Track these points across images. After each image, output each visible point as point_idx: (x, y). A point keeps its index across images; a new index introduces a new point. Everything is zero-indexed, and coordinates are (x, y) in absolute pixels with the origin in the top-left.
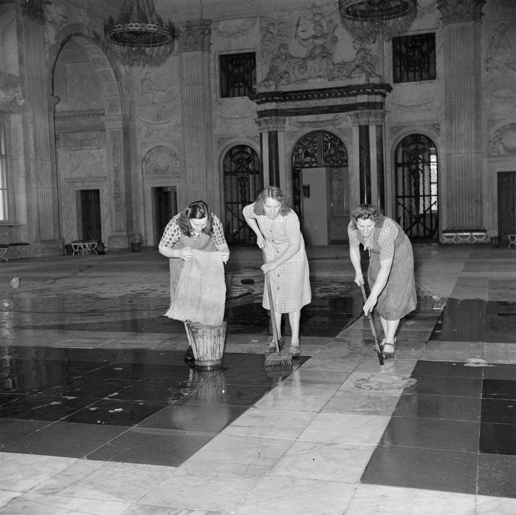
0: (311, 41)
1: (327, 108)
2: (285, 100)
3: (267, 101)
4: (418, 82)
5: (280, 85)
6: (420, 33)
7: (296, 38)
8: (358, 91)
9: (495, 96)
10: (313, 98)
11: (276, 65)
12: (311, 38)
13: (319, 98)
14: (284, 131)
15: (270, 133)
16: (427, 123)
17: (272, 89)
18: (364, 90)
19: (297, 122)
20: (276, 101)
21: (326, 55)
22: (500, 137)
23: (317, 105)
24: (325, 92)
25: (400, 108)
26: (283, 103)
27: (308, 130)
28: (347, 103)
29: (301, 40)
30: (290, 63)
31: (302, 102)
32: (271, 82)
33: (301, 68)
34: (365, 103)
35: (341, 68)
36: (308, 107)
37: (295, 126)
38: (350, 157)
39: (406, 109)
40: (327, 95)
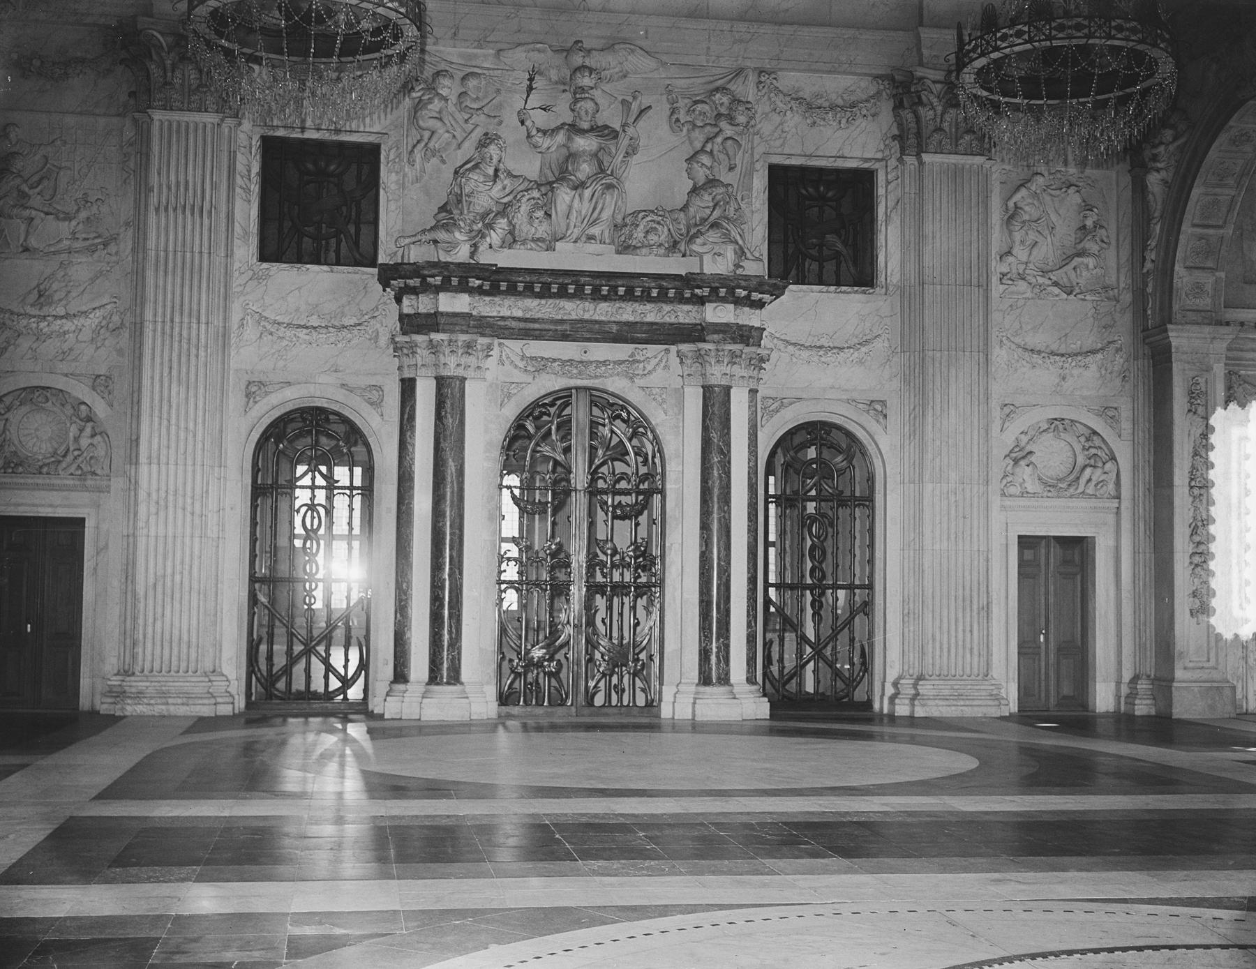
0: (561, 137)
1: (615, 328)
2: (494, 291)
3: (445, 287)
4: (833, 288)
5: (483, 247)
6: (840, 164)
7: (522, 123)
8: (714, 290)
9: (1019, 346)
10: (579, 294)
11: (467, 190)
12: (562, 132)
13: (597, 296)
14: (485, 379)
15: (441, 382)
16: (855, 395)
17: (462, 254)
18: (731, 291)
19: (523, 357)
20: (471, 291)
21: (615, 182)
22: (1029, 448)
23: (587, 316)
24: (583, 280)
25: (791, 348)
26: (487, 299)
27: (551, 383)
28: (673, 320)
29: (534, 132)
30: (504, 188)
31: (543, 302)
32: (457, 234)
33: (536, 207)
34: (727, 325)
35: (659, 223)
36: (559, 317)
37: (516, 366)
38: (672, 468)
39: (805, 354)
40: (621, 290)
